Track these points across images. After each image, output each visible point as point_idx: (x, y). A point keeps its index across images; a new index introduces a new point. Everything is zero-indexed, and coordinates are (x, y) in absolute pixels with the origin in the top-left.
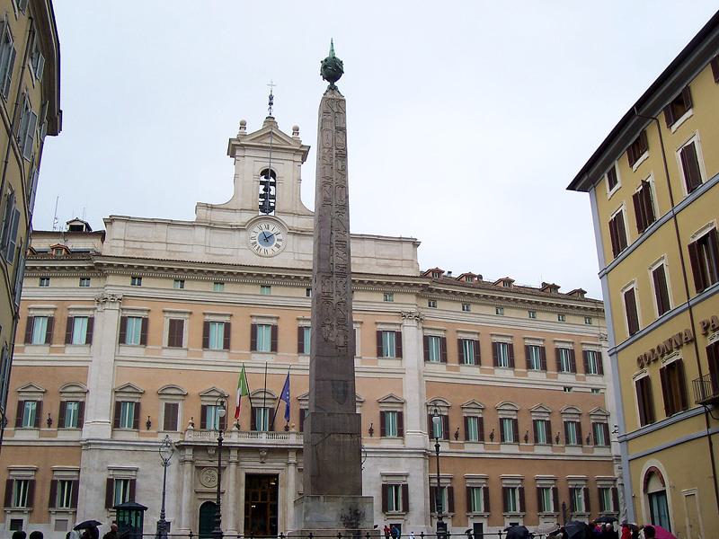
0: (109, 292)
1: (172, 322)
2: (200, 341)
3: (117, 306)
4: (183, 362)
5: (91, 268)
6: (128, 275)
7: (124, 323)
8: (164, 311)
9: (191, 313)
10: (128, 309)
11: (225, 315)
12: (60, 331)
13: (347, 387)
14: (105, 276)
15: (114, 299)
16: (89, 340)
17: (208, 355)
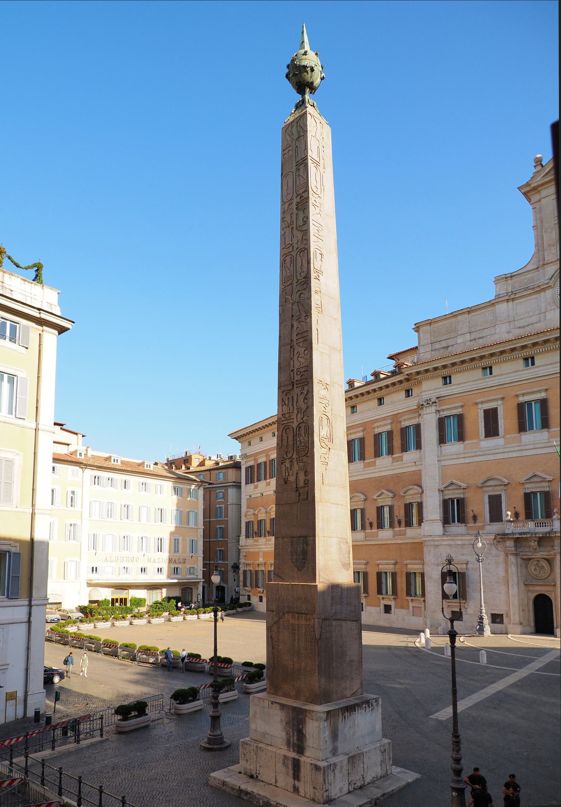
0: (425, 396)
1: (486, 412)
2: (516, 426)
3: (433, 409)
4: (501, 450)
5: (408, 380)
6: (438, 377)
7: (441, 423)
8: (476, 404)
9: (503, 399)
10: (443, 410)
11: (539, 391)
12: (397, 443)
13: (307, 545)
14: (420, 383)
15: (429, 403)
16: (419, 446)
17: (527, 437)
